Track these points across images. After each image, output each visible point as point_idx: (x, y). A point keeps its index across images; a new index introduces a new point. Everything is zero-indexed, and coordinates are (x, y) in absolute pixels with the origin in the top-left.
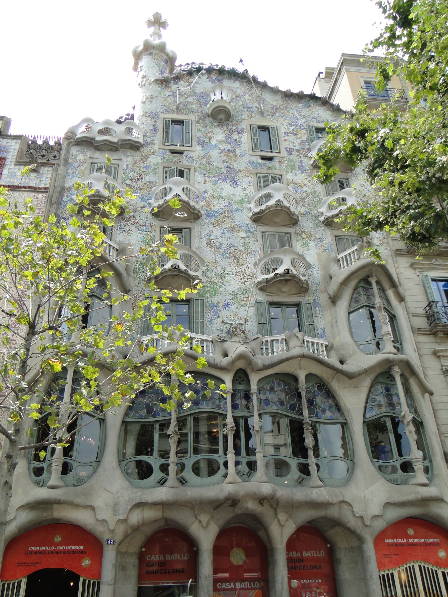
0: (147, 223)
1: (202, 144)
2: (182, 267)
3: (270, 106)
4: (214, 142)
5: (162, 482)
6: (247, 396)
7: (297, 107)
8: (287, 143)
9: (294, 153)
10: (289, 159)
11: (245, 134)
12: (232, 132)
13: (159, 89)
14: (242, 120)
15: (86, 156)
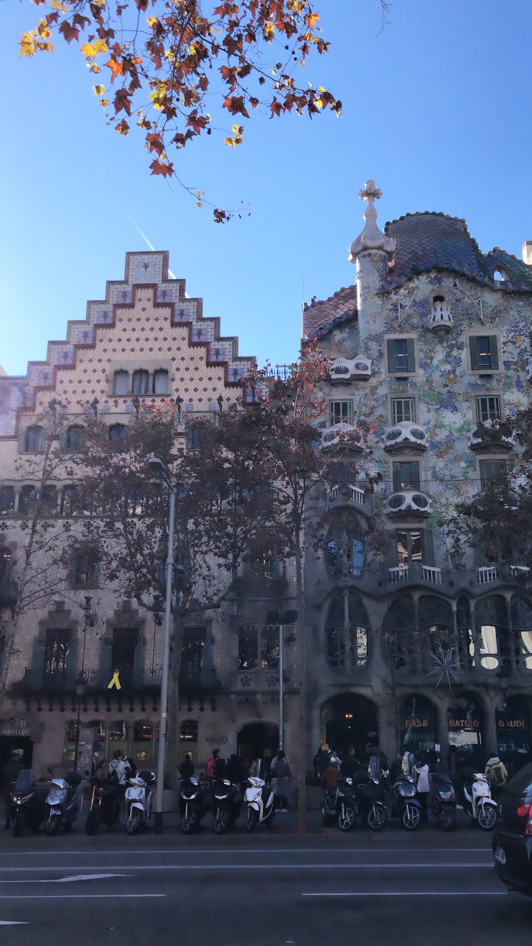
0: (382, 459)
1: (424, 366)
2: (415, 507)
3: (490, 309)
4: (435, 362)
5: (414, 672)
6: (468, 614)
7: (518, 305)
8: (506, 355)
9: (512, 367)
10: (507, 376)
11: (465, 349)
12: (451, 347)
13: (381, 302)
14: (462, 331)
15: (324, 393)
